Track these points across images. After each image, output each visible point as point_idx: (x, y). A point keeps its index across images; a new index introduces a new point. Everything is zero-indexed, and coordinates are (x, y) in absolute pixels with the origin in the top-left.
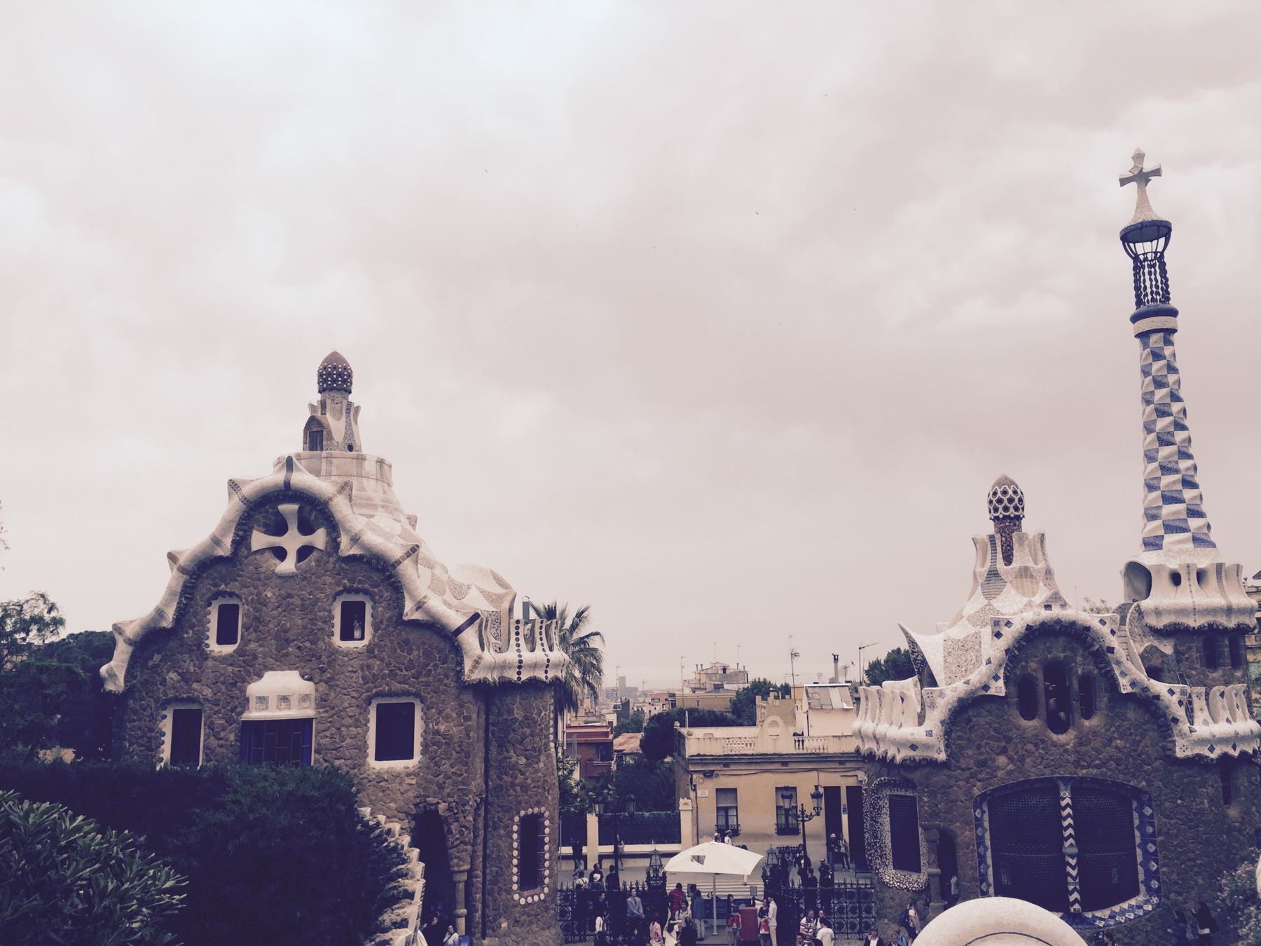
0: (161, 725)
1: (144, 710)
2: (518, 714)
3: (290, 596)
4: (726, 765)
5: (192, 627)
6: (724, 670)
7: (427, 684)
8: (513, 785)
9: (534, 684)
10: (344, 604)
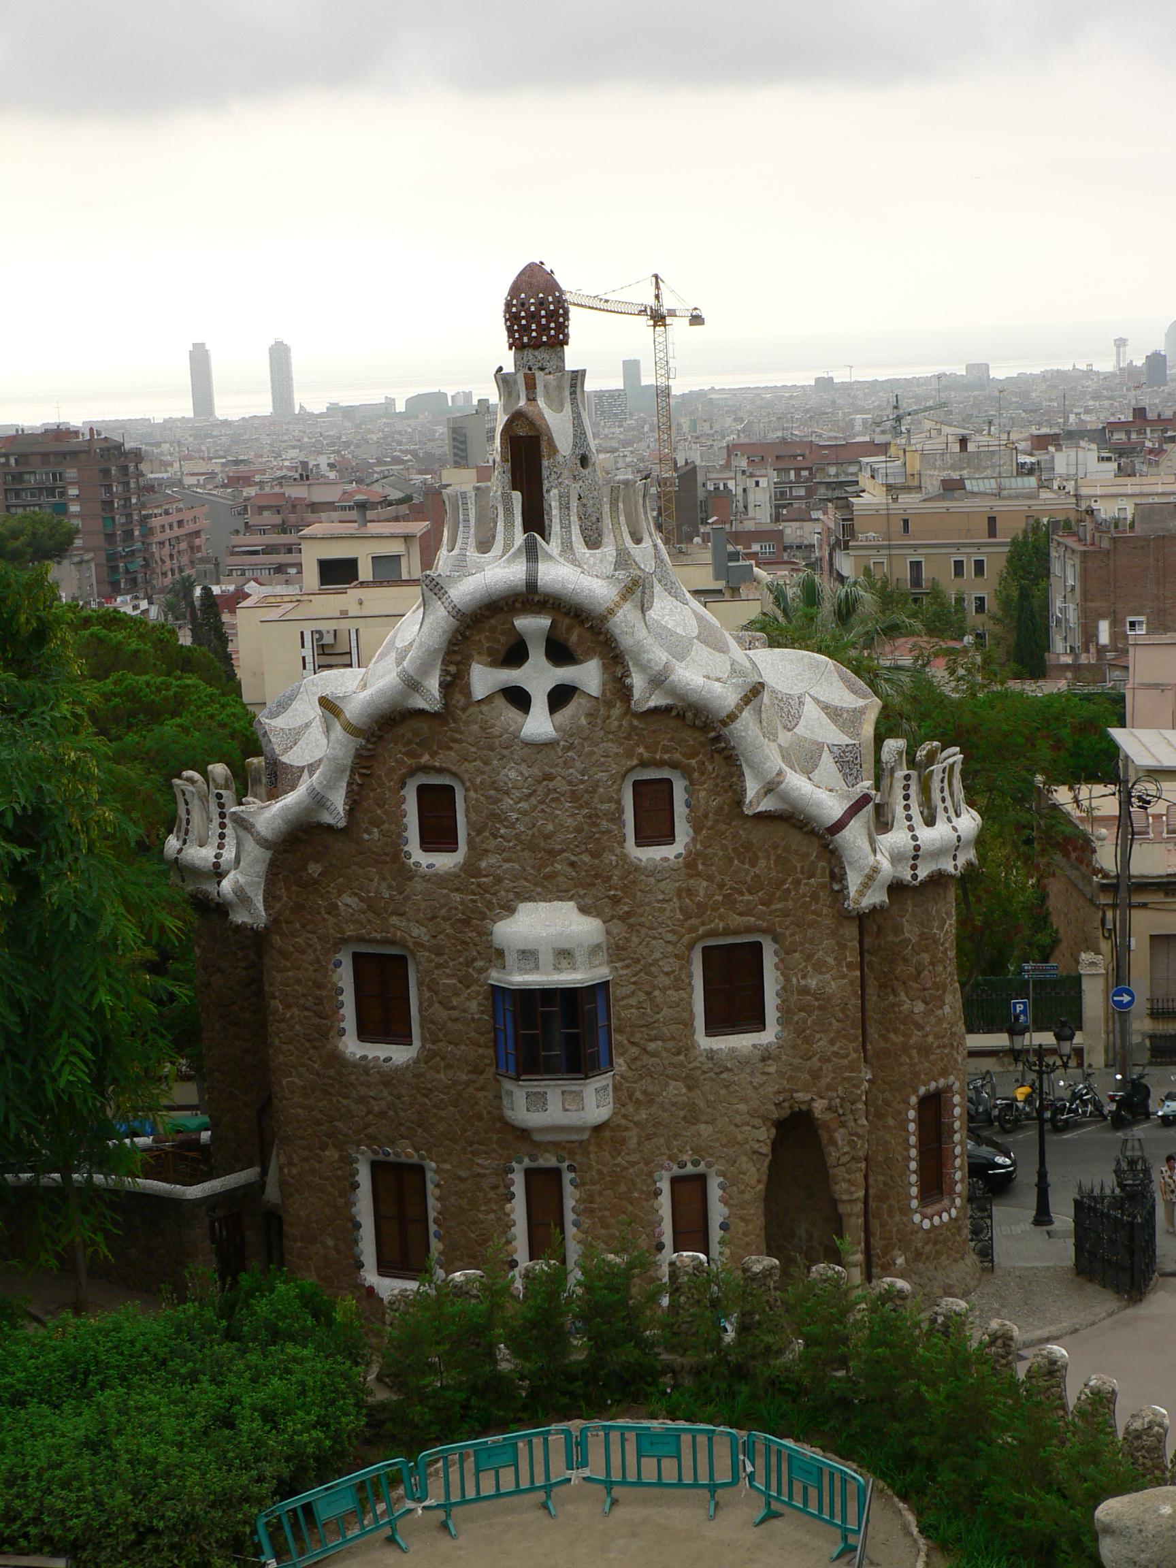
0: (335, 978)
1: (303, 952)
2: (911, 932)
3: (549, 777)
4: (1167, 894)
5: (377, 823)
6: (963, 442)
7: (786, 914)
8: (905, 1049)
9: (938, 880)
10: (636, 784)
